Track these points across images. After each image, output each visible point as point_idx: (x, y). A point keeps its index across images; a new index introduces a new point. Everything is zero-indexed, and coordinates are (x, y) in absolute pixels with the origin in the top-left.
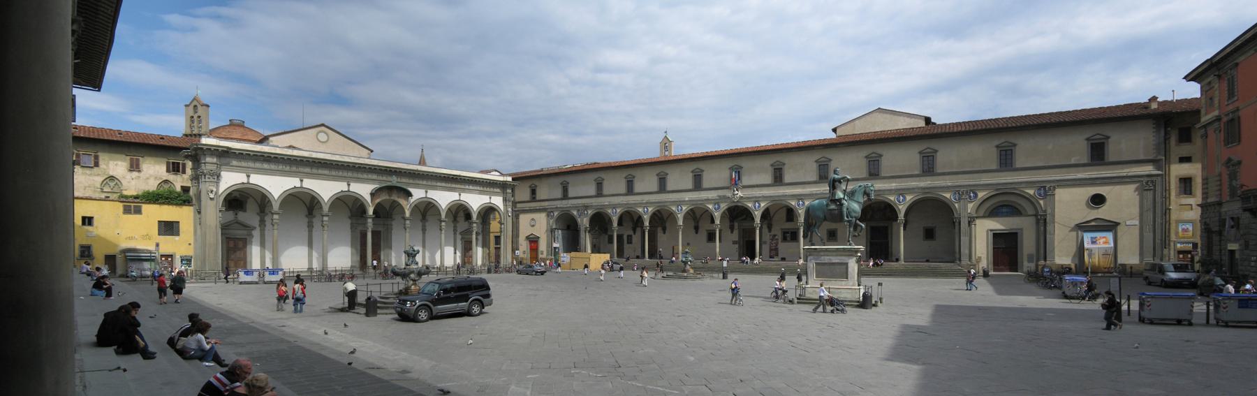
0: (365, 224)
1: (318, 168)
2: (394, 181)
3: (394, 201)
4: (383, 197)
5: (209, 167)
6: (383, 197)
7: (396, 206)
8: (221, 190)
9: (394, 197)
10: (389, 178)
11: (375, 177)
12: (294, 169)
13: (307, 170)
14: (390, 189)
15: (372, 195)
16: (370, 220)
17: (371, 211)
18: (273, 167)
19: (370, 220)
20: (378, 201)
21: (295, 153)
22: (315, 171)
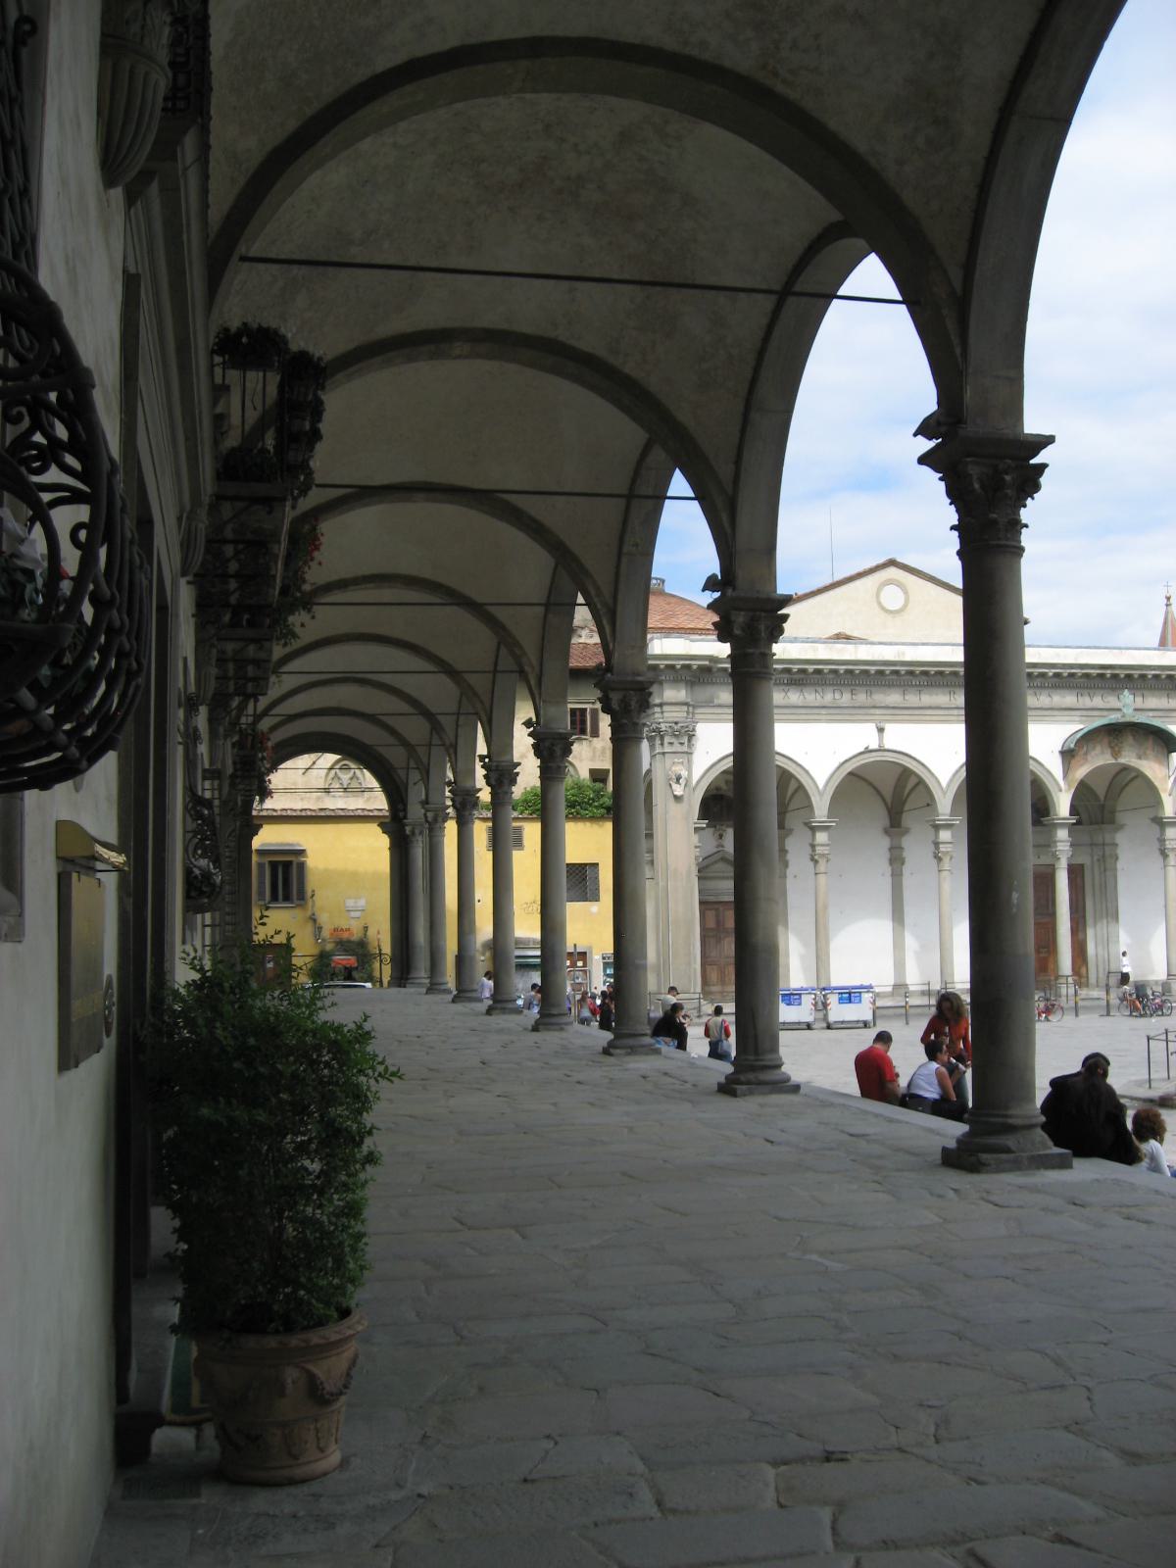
0: (1047, 845)
1: (920, 688)
2: (1128, 706)
3: (1125, 769)
4: (1099, 759)
5: (673, 714)
6: (1099, 759)
7: (1125, 780)
8: (696, 777)
9: (1129, 758)
10: (1112, 701)
11: (1069, 699)
12: (862, 698)
13: (894, 698)
14: (1114, 733)
15: (1068, 755)
16: (1062, 834)
17: (1063, 804)
18: (810, 697)
19: (1062, 834)
20: (1081, 772)
21: (863, 653)
22: (912, 699)
